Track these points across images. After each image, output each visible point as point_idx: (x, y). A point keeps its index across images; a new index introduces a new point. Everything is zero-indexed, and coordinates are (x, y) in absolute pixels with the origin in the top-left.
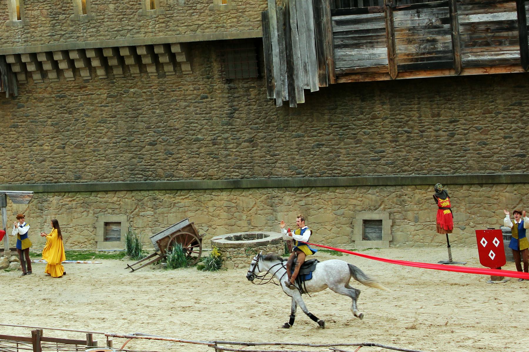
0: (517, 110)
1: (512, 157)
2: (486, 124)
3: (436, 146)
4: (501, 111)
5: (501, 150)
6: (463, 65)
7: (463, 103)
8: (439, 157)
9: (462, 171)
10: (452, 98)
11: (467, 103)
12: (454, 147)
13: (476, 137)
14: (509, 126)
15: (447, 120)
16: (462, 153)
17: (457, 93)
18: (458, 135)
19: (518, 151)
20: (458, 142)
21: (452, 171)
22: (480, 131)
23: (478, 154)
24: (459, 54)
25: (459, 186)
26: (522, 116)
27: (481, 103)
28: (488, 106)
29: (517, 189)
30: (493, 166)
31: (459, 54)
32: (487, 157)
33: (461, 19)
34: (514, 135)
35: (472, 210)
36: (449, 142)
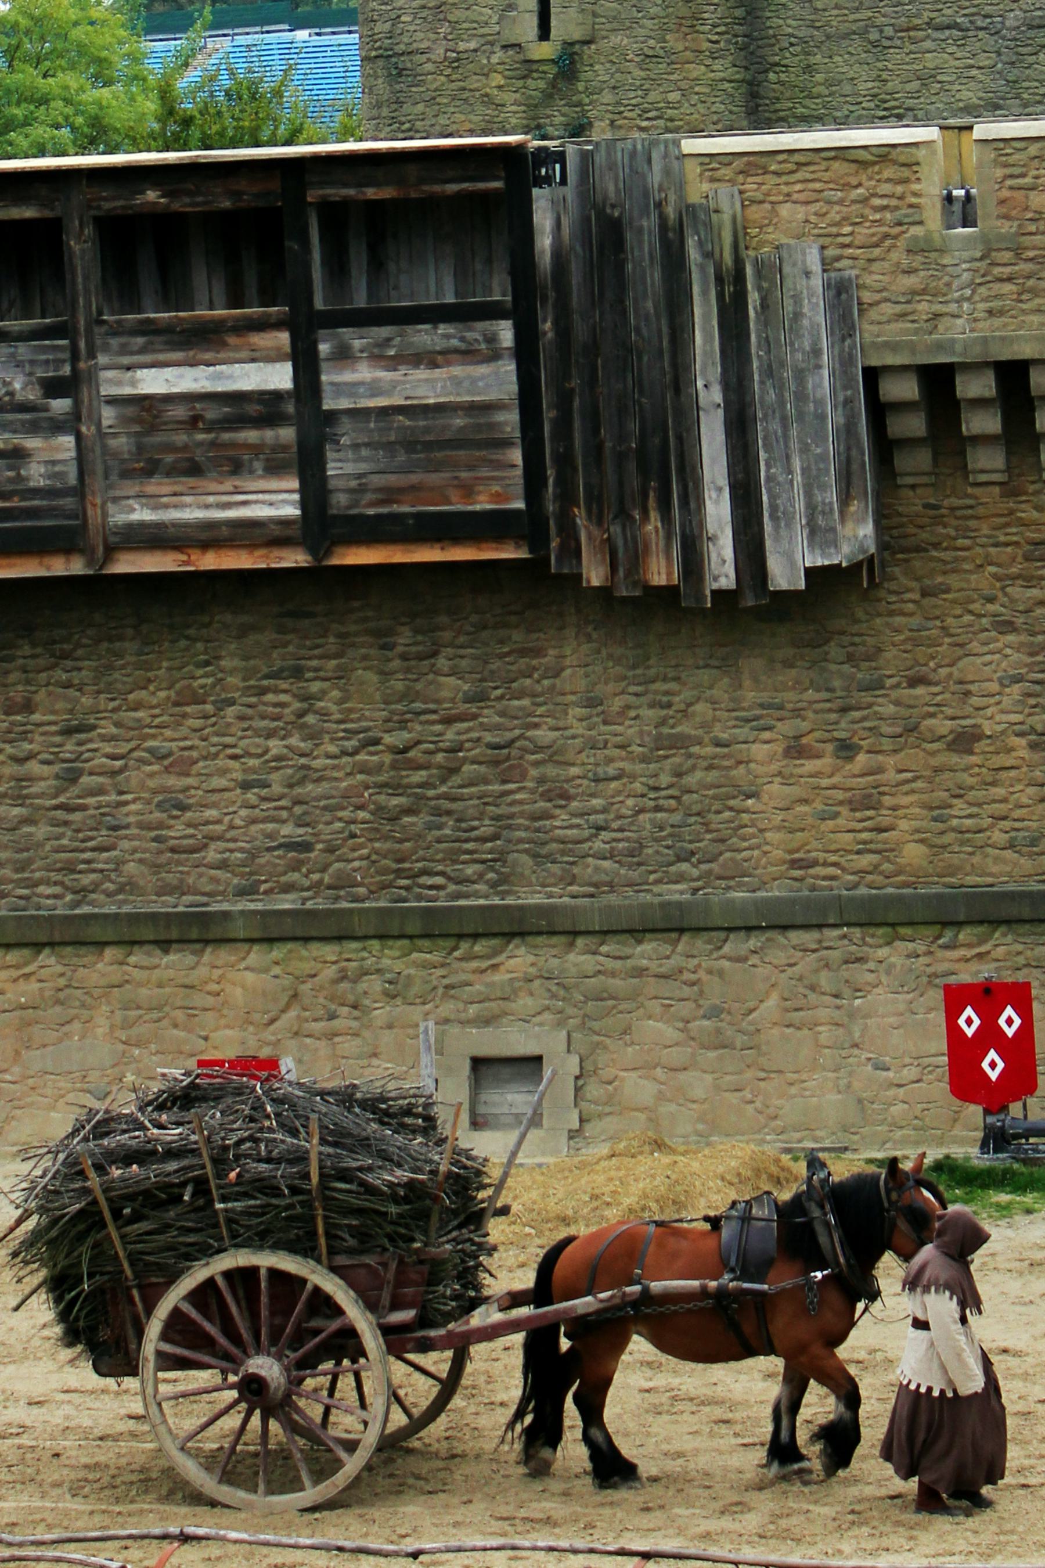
0: (285, 691)
1: (269, 849)
2: (185, 739)
3: (16, 811)
4: (237, 695)
5: (232, 827)
6: (112, 539)
7: (110, 667)
8: (27, 850)
9: (102, 897)
10: (75, 649)
11: (123, 667)
12: (77, 817)
13: (151, 783)
14: (258, 746)
15: (55, 723)
16: (102, 837)
17: (89, 632)
18: (91, 774)
19: (287, 830)
20: (91, 801)
21: (69, 897)
22: (166, 762)
23: (155, 839)
24: (99, 501)
25: (92, 949)
26: (301, 714)
27: (169, 669)
28: (193, 678)
29: (283, 960)
30: (204, 880)
31: (99, 501)
32: (184, 852)
33: (110, 381)
34: (275, 776)
35: (135, 1031)
36: (62, 799)
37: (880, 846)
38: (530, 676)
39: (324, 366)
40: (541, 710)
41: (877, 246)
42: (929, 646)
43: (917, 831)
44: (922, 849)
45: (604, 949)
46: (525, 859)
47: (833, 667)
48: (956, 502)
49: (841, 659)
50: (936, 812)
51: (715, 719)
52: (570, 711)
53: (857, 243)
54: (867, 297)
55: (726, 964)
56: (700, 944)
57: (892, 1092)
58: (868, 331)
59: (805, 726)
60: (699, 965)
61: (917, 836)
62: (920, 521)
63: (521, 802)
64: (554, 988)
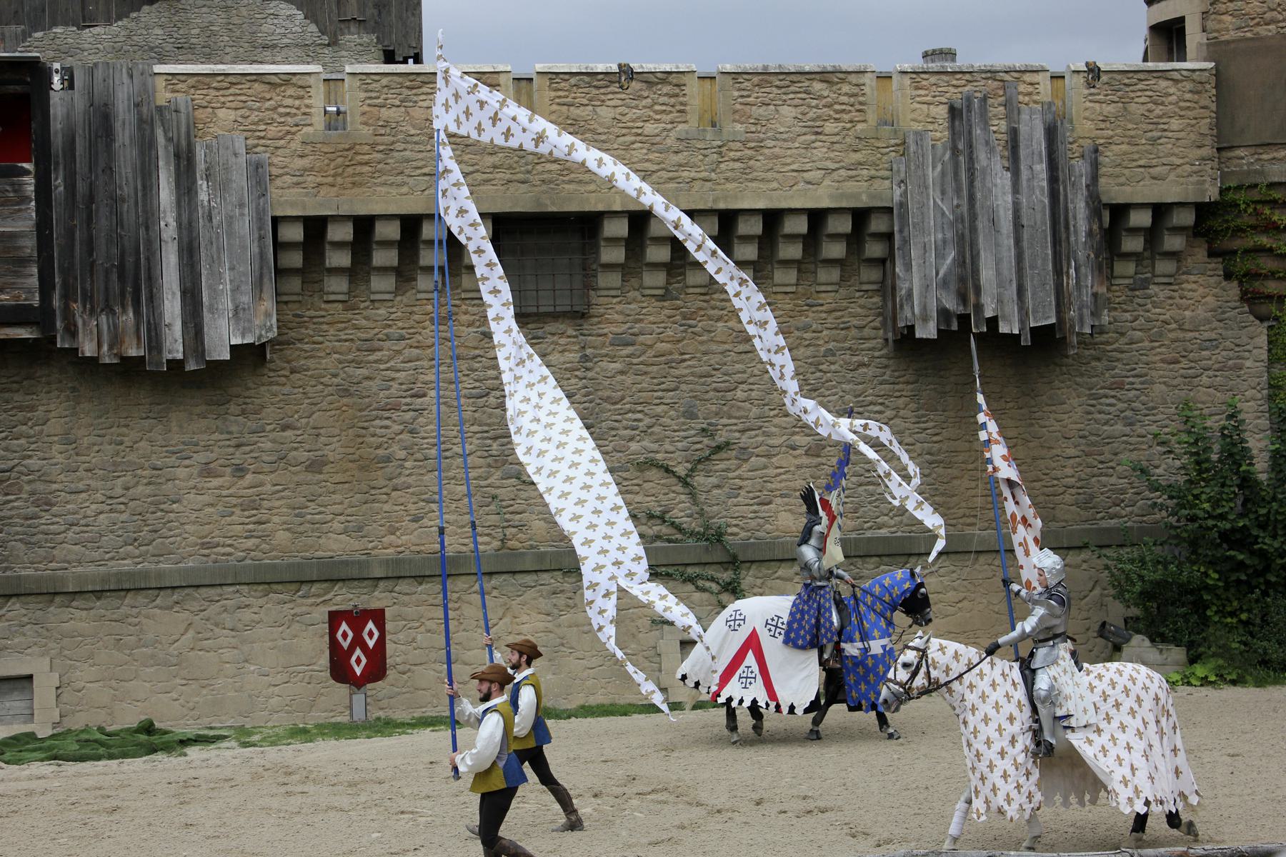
37: (260, 533)
38: (25, 424)
40: (33, 447)
41: (282, 139)
42: (295, 405)
43: (285, 523)
44: (288, 534)
45: (74, 604)
46: (19, 545)
47: (232, 418)
48: (312, 313)
49: (237, 413)
50: (297, 511)
51: (152, 452)
52: (54, 448)
53: (269, 136)
54: (275, 171)
55: (157, 611)
56: (141, 599)
57: (271, 689)
58: (274, 192)
59: (213, 456)
60: (140, 613)
61: (285, 526)
62: (290, 325)
63: (18, 508)
64: (40, 630)
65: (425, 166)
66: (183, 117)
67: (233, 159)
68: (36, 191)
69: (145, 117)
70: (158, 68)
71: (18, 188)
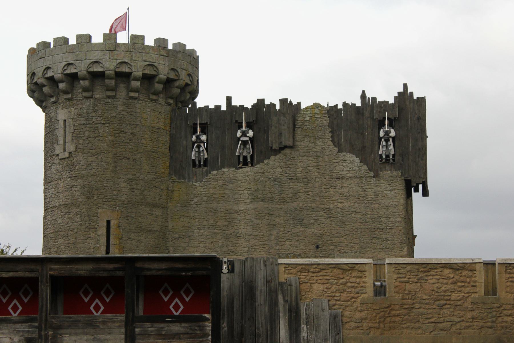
39: (138, 337)
54: (345, 320)
65: (432, 317)
66: (294, 288)
67: (321, 313)
68: (212, 330)
69: (272, 288)
70: (281, 261)
71: (202, 328)
